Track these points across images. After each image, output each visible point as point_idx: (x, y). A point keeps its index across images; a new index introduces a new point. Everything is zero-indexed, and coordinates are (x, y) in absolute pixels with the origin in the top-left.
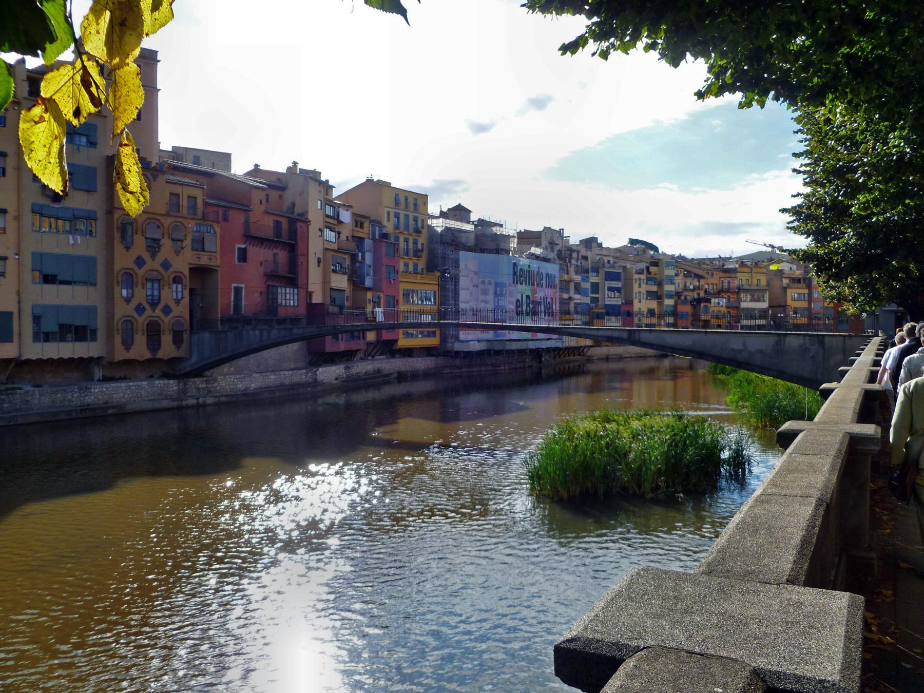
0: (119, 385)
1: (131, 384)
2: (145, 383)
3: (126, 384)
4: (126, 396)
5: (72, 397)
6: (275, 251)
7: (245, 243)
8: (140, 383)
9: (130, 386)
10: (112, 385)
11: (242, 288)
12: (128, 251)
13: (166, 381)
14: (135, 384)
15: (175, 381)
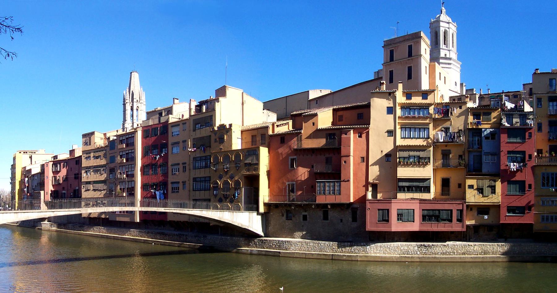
0: (218, 237)
1: (223, 237)
2: (229, 238)
3: (221, 237)
4: (221, 243)
5: (201, 239)
6: (327, 155)
7: (296, 155)
8: (226, 237)
9: (223, 238)
10: (215, 237)
11: (294, 184)
12: (216, 172)
13: (239, 238)
14: (225, 237)
15: (243, 239)
